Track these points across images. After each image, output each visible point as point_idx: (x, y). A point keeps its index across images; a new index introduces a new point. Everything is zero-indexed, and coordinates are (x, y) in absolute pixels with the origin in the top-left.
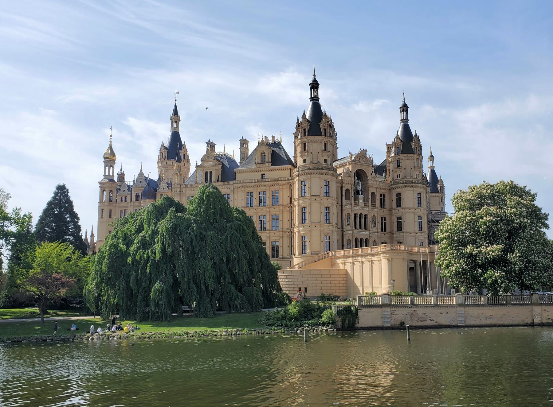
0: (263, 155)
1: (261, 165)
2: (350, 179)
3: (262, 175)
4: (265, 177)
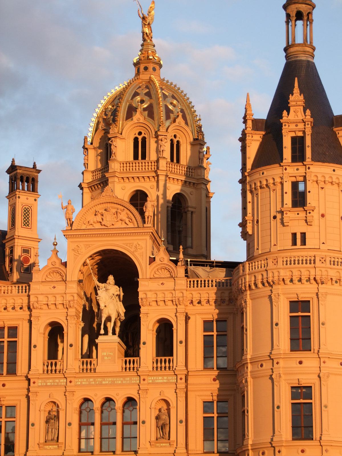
2: (60, 288)
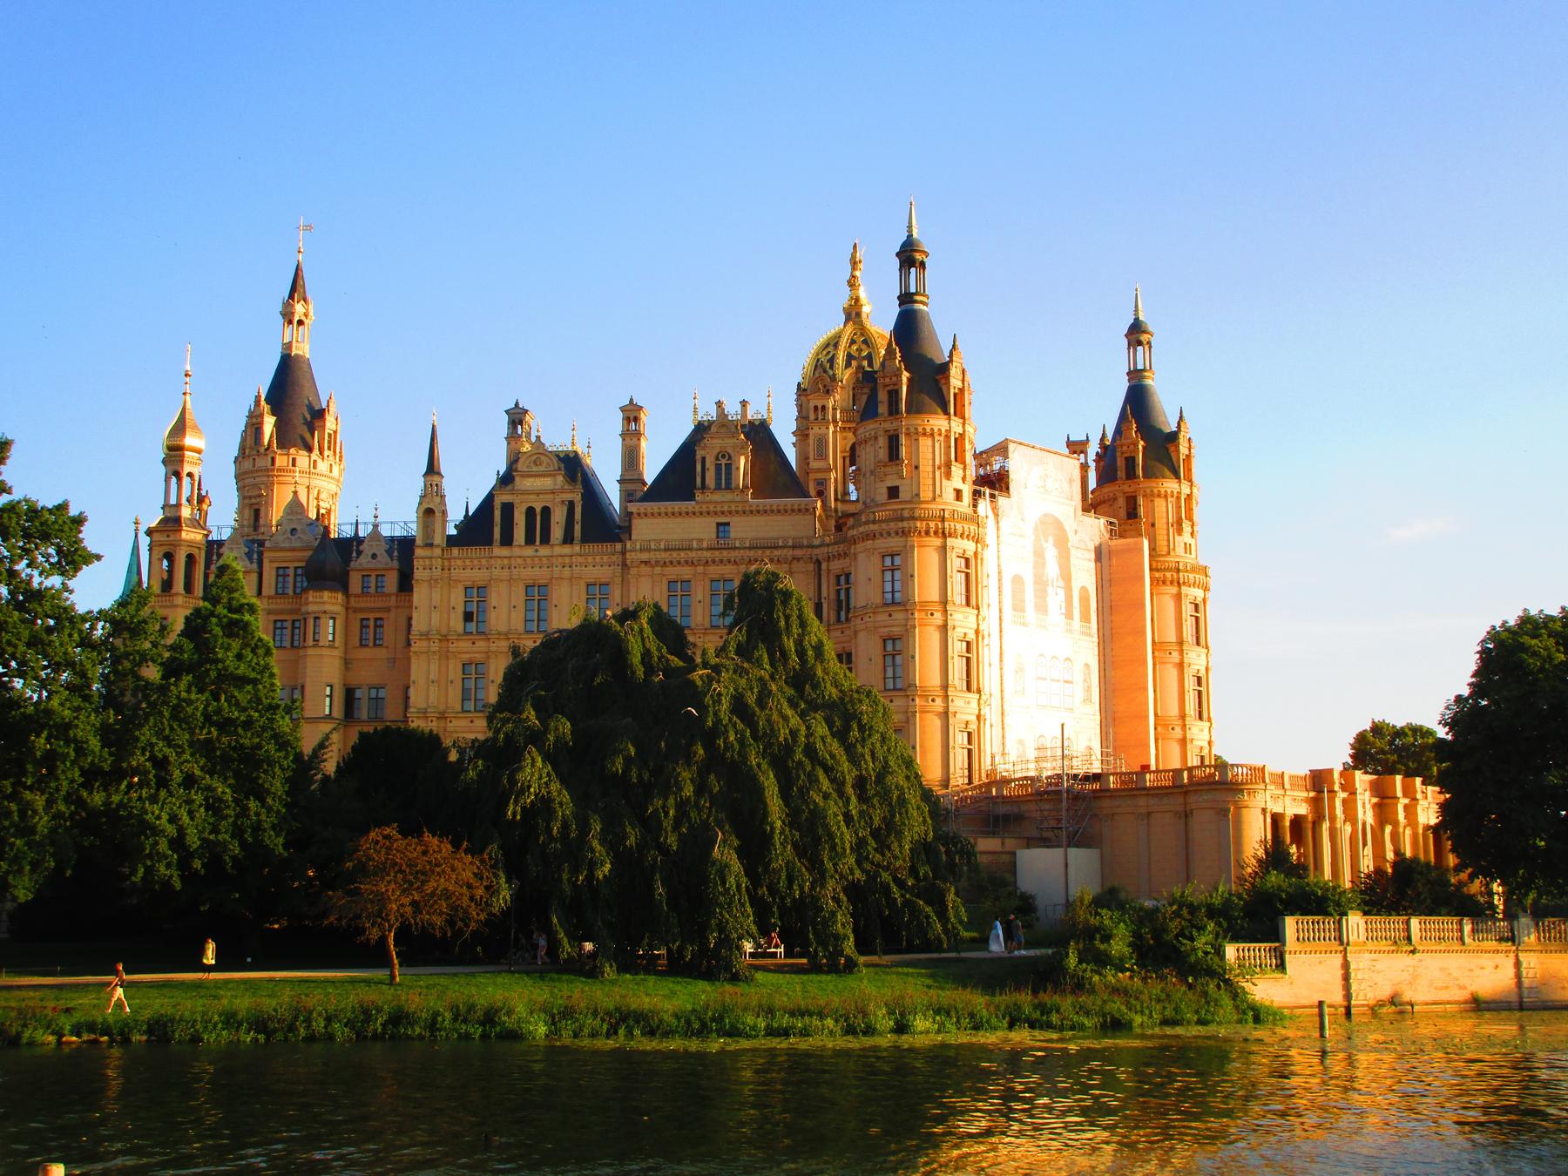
0: (723, 462)
1: (717, 497)
3: (719, 524)
4: (732, 535)
